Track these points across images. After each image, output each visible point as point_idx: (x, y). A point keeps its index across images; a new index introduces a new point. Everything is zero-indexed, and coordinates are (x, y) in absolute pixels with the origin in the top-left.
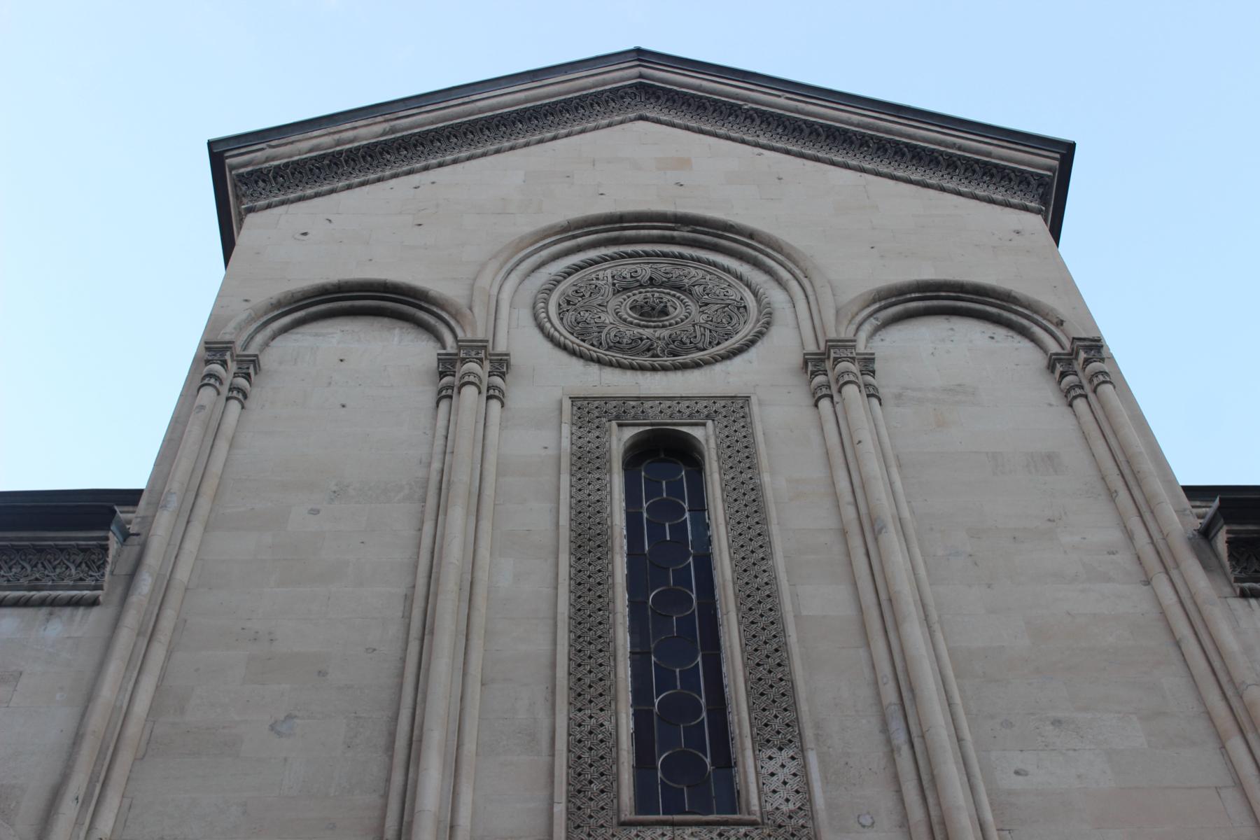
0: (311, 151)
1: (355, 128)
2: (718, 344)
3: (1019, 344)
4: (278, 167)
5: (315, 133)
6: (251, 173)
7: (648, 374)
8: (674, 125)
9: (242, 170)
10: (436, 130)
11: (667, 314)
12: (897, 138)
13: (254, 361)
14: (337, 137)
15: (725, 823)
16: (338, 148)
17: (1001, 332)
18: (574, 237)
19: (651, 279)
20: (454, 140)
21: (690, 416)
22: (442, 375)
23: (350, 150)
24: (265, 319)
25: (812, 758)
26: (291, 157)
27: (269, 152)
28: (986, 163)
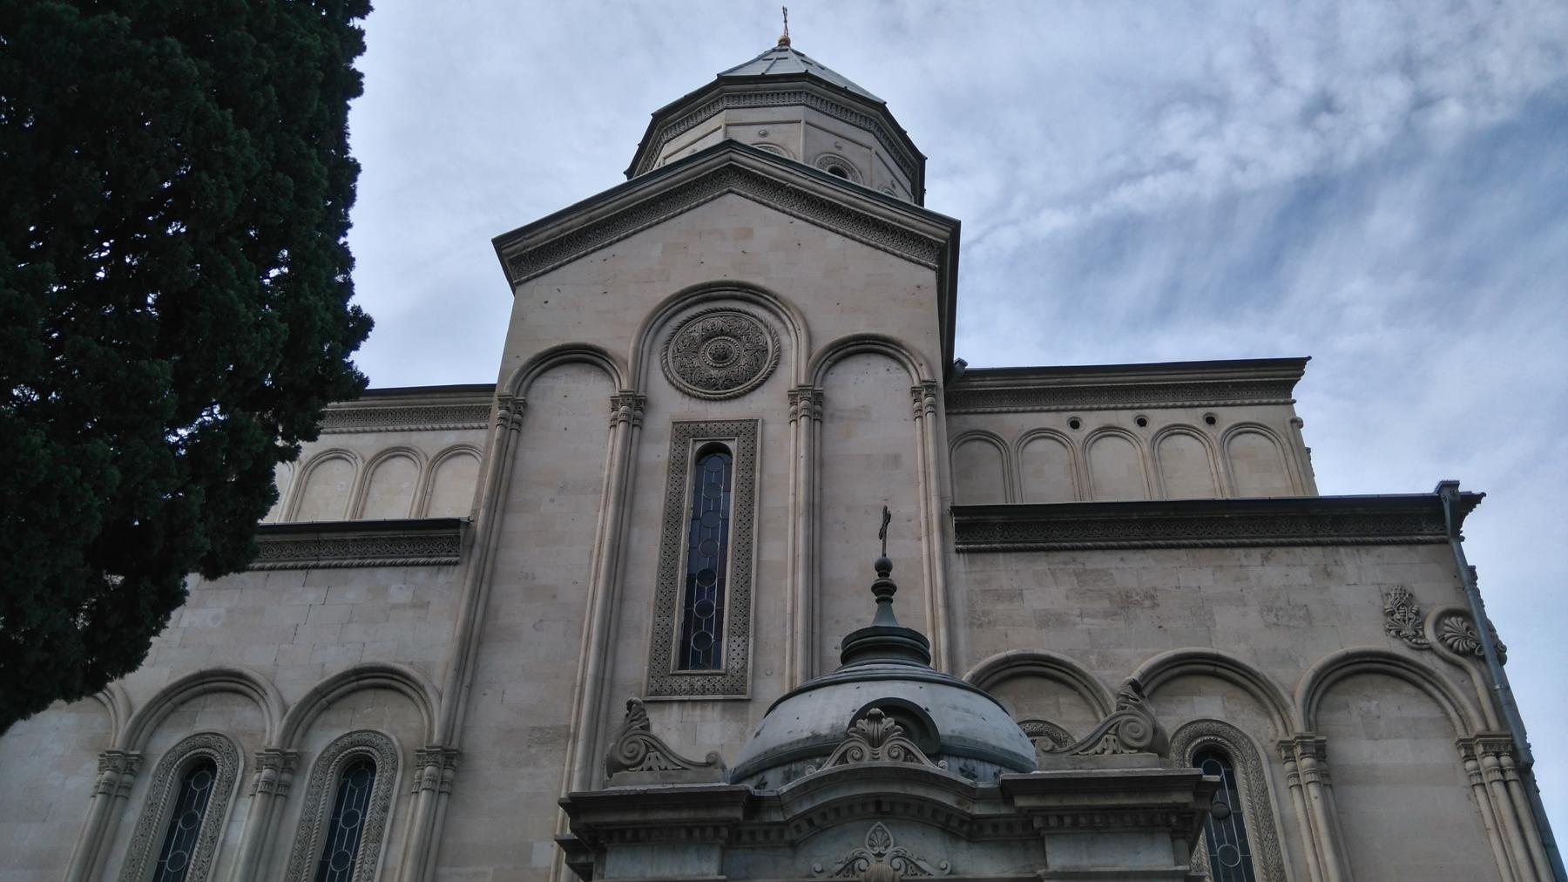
0: (548, 238)
1: (570, 220)
2: (750, 379)
3: (902, 375)
4: (530, 252)
5: (549, 226)
7: (713, 403)
8: (747, 198)
9: (512, 257)
11: (727, 358)
12: (866, 213)
13: (525, 404)
14: (561, 227)
15: (712, 675)
16: (562, 235)
17: (894, 365)
18: (686, 299)
19: (722, 330)
22: (613, 410)
24: (527, 372)
25: (751, 640)
26: (537, 244)
27: (525, 242)
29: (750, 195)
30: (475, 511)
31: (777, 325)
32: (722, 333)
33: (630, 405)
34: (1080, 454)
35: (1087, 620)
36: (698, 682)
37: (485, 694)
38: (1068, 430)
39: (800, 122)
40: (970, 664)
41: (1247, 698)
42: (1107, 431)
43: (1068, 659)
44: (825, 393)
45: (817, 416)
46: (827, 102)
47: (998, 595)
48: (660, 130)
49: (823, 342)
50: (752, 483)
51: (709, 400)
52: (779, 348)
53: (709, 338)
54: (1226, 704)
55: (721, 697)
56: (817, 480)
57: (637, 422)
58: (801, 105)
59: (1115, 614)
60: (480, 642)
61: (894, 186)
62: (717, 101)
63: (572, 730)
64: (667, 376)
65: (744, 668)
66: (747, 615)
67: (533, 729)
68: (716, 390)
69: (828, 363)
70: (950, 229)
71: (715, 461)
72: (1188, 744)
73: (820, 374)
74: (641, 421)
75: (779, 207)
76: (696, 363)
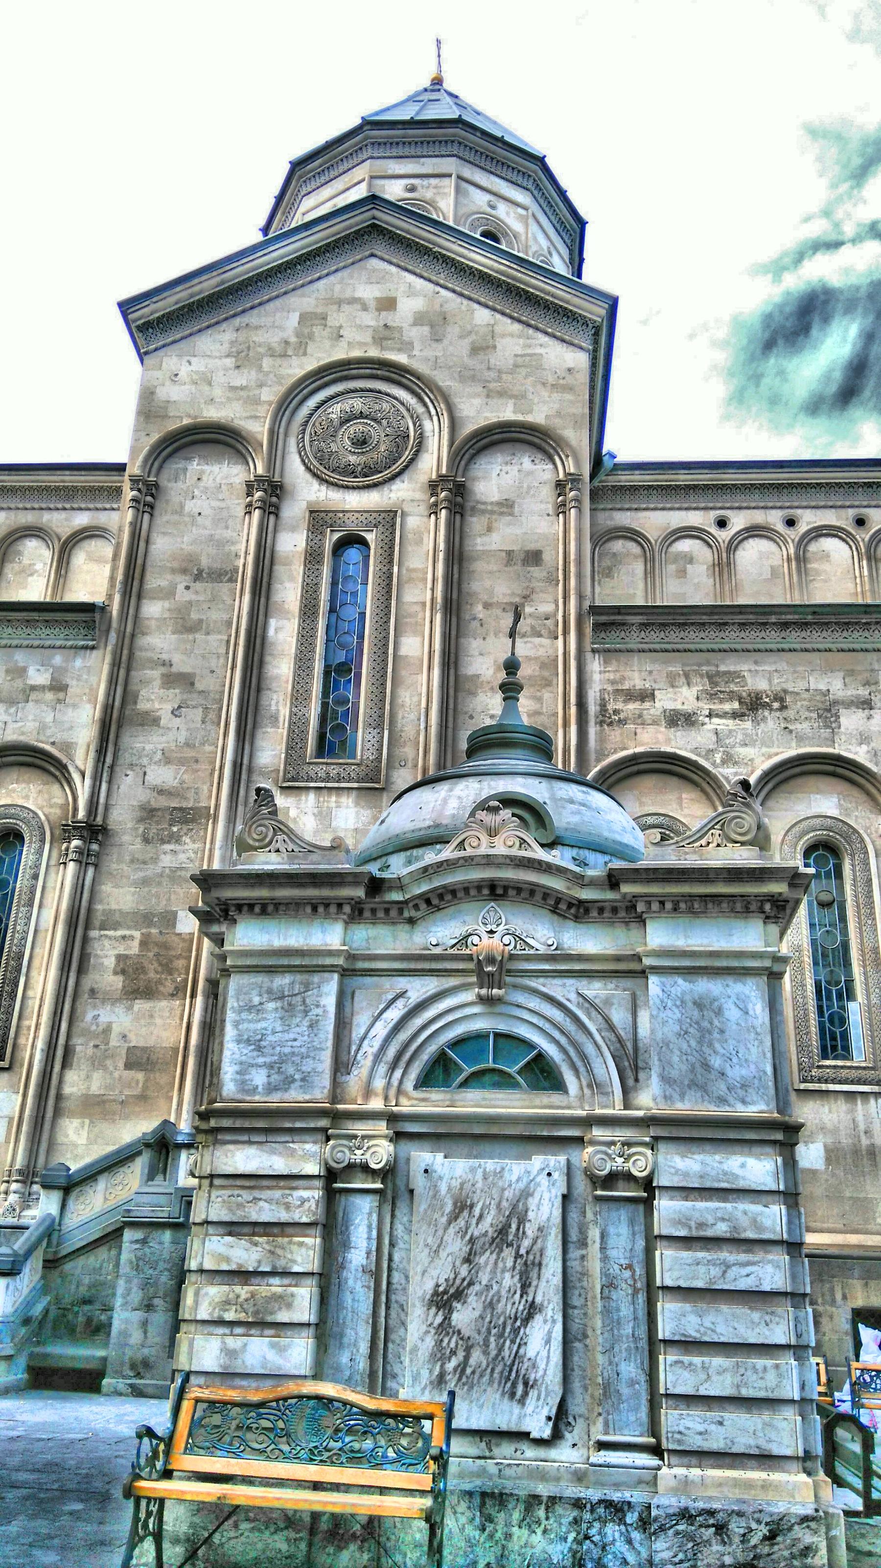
0: (176, 303)
4: (158, 318)
6: (144, 324)
10: (249, 279)
13: (156, 485)
14: (190, 291)
17: (540, 456)
20: (259, 284)
21: (366, 525)
22: (248, 495)
23: (198, 300)
27: (153, 307)
28: (566, 309)
29: (395, 260)
30: (110, 597)
31: (420, 409)
32: (361, 415)
33: (265, 491)
34: (724, 555)
35: (715, 720)
36: (334, 771)
37: (127, 775)
38: (714, 530)
39: (450, 176)
40: (598, 760)
41: (863, 797)
42: (754, 531)
43: (694, 757)
44: (468, 484)
45: (458, 509)
46: (482, 153)
47: (631, 695)
48: (298, 180)
49: (467, 429)
50: (390, 577)
51: (347, 487)
52: (421, 434)
53: (348, 421)
54: (842, 802)
55: (355, 785)
56: (456, 576)
57: (272, 509)
58: (453, 156)
59: (743, 715)
60: (119, 727)
61: (550, 254)
62: (361, 149)
63: (212, 812)
64: (303, 461)
65: (379, 759)
66: (382, 708)
67: (175, 808)
68: (356, 477)
69: (471, 451)
70: (606, 306)
71: (353, 554)
72: (801, 838)
73: (463, 463)
74: (277, 508)
75: (426, 275)
76: (334, 447)
